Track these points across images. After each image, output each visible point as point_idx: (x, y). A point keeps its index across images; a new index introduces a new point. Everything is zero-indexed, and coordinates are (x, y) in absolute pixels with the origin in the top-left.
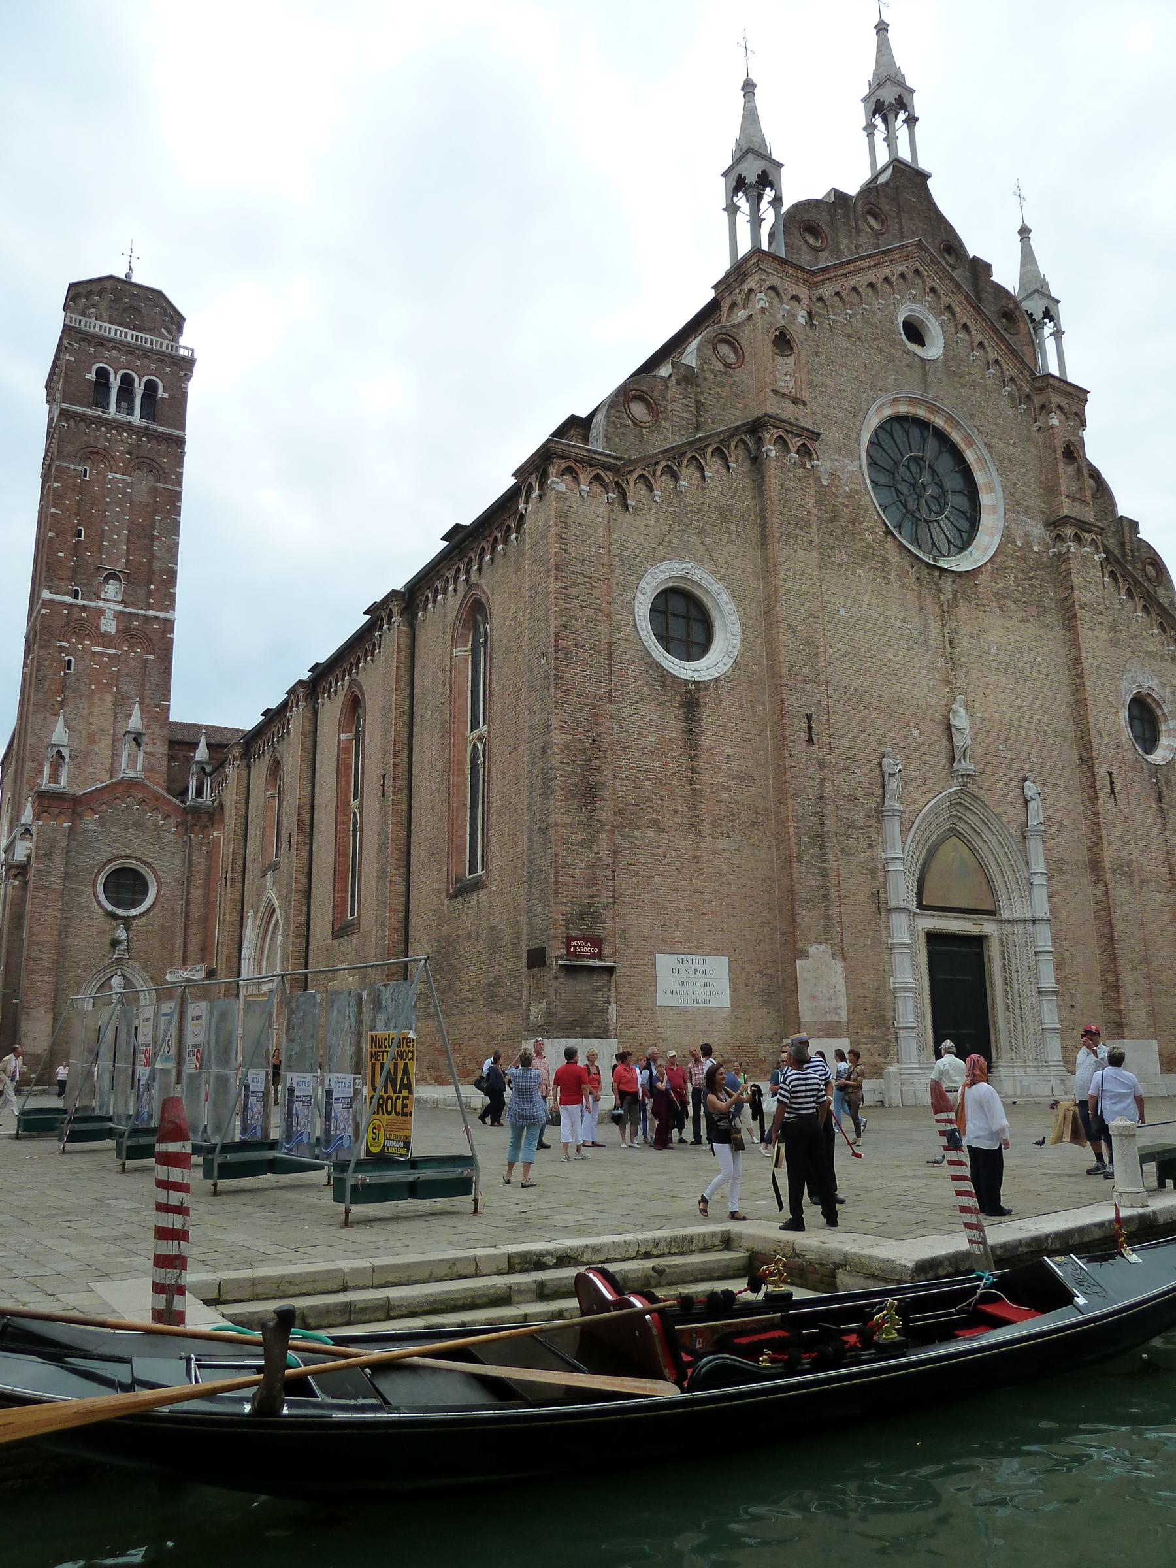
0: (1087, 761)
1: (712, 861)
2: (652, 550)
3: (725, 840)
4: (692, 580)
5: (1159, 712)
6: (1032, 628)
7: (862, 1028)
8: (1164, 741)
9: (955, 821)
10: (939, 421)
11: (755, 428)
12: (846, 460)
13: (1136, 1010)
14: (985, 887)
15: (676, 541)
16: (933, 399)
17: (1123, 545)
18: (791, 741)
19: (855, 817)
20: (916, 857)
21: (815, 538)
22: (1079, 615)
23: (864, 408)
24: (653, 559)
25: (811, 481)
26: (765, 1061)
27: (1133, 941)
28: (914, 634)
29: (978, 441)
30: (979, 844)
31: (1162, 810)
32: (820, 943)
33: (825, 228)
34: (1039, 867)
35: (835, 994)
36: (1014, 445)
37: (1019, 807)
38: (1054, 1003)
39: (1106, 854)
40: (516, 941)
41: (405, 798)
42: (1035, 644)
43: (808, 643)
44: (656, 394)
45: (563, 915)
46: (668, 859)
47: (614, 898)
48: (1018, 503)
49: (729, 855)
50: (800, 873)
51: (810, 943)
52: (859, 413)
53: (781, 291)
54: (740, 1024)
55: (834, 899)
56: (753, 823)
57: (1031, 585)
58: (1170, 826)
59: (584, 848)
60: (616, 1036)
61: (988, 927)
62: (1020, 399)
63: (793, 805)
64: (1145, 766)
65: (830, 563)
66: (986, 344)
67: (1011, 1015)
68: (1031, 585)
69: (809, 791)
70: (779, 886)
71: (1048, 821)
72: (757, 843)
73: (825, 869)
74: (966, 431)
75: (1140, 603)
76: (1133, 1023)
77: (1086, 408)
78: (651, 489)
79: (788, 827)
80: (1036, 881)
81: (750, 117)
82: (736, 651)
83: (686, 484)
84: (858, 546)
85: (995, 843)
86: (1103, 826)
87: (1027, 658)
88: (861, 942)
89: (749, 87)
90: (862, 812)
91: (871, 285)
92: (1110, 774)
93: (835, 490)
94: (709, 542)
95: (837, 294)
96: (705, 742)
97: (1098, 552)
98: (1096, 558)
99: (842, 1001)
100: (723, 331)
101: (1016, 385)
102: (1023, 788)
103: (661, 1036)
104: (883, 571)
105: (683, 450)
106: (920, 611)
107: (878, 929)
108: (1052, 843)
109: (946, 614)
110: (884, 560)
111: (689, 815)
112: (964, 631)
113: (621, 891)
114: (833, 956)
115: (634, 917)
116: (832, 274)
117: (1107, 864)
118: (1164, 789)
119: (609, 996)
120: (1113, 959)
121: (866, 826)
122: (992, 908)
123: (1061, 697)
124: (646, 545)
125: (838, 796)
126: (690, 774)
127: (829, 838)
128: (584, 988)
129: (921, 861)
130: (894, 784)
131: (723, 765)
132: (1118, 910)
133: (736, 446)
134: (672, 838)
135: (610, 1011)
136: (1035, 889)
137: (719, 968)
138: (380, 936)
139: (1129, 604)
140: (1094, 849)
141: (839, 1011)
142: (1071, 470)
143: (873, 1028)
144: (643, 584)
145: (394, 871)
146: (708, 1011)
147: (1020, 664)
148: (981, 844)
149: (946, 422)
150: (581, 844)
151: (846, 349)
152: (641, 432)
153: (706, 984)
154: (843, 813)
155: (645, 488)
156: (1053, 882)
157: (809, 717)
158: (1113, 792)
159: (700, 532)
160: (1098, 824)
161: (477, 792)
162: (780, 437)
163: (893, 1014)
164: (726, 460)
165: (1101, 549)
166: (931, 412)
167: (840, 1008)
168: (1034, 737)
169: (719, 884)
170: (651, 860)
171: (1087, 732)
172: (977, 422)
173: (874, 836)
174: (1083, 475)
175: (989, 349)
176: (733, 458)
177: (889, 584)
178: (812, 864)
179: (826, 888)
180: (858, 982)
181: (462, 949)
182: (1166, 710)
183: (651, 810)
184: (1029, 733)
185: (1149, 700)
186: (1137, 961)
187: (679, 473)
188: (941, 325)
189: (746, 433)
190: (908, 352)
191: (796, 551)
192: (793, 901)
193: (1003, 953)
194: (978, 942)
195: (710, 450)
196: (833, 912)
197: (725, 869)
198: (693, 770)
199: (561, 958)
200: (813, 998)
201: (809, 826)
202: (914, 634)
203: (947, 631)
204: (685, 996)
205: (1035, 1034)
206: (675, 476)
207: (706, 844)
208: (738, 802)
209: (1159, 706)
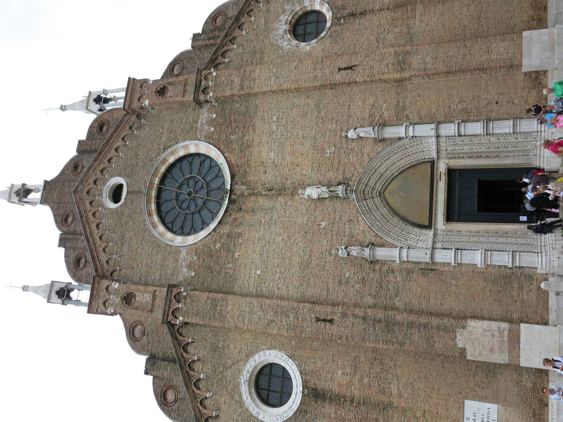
1: (405, 399)
2: (237, 403)
4: (250, 378)
5: (300, 13)
6: (258, 123)
7: (512, 297)
8: (317, 7)
10: (157, 181)
11: (171, 326)
12: (181, 256)
14: (415, 170)
15: (231, 385)
16: (146, 189)
17: (206, 46)
18: (332, 336)
21: (221, 295)
22: (247, 92)
23: (155, 239)
24: (241, 403)
25: (192, 293)
26: (534, 383)
27: (450, 53)
28: (268, 217)
29: (163, 156)
30: (388, 174)
32: (456, 337)
33: (76, 254)
35: (490, 331)
36: (163, 128)
37: (364, 142)
39: (391, 76)
42: (266, 121)
43: (276, 312)
44: (162, 383)
48: (192, 128)
49: (402, 384)
50: (411, 345)
51: (455, 345)
52: (158, 245)
53: (105, 299)
54: (508, 398)
56: (381, 363)
57: (235, 122)
58: (371, 7)
61: (442, 167)
62: (139, 122)
63: (369, 342)
64: (333, 29)
65: (234, 277)
66: (115, 146)
67: (503, 154)
68: (235, 122)
69: (361, 328)
72: (393, 362)
73: (408, 325)
74: (159, 164)
75: (237, 32)
76: (510, 55)
77: (138, 79)
78: (206, 398)
80: (411, 134)
81: (36, 290)
82: (285, 356)
83: (202, 375)
84: (223, 254)
85: (388, 162)
87: (275, 128)
88: (454, 289)
89: (25, 288)
90: (372, 275)
91: (97, 226)
92: (340, 69)
93: (197, 267)
94: (229, 362)
95: (104, 250)
96: (335, 389)
97: (211, 73)
98: (214, 74)
99: (494, 325)
100: (128, 333)
101: (133, 125)
102: (352, 139)
104: (235, 237)
105: (186, 374)
106: (254, 212)
107: (445, 273)
109: (256, 191)
110: (229, 236)
111: (378, 411)
112: (263, 178)
114: (464, 328)
116: (95, 254)
117: (398, 76)
118: (347, 11)
121: (380, 274)
122: (429, 164)
123: (295, 100)
124: (234, 406)
125: (363, 293)
126: (354, 404)
127: (388, 317)
131: (349, 378)
133: (181, 335)
136: (416, 134)
139: (239, 40)
141: (502, 329)
142: (170, 88)
143: (512, 287)
144: (254, 413)
147: (279, 134)
148: (388, 172)
149: (156, 176)
151: (128, 247)
152: (181, 399)
155: (206, 401)
156: (411, 116)
157: (318, 320)
158: (350, 68)
159: (225, 368)
162: (172, 313)
163: (503, 269)
164: (188, 344)
165: (209, 71)
166: (153, 187)
167: (499, 328)
168: (321, 125)
169: (419, 396)
171: (315, 87)
172: (153, 156)
173: (386, 267)
174: (172, 82)
175: (118, 144)
176: (187, 339)
177: (241, 234)
178: (405, 334)
179: (420, 325)
180: (481, 296)
182: (299, 8)
184: (318, 130)
185: (294, 21)
187: (198, 378)
188: (111, 177)
189: (173, 327)
190: (125, 203)
191: (228, 312)
193: (459, 158)
194: (451, 172)
195: (184, 354)
197: (409, 390)
201: (382, 332)
202: (268, 217)
203: (263, 193)
205: (517, 138)
206: (199, 380)
207: (395, 401)
208: (370, 372)
209: (296, 13)
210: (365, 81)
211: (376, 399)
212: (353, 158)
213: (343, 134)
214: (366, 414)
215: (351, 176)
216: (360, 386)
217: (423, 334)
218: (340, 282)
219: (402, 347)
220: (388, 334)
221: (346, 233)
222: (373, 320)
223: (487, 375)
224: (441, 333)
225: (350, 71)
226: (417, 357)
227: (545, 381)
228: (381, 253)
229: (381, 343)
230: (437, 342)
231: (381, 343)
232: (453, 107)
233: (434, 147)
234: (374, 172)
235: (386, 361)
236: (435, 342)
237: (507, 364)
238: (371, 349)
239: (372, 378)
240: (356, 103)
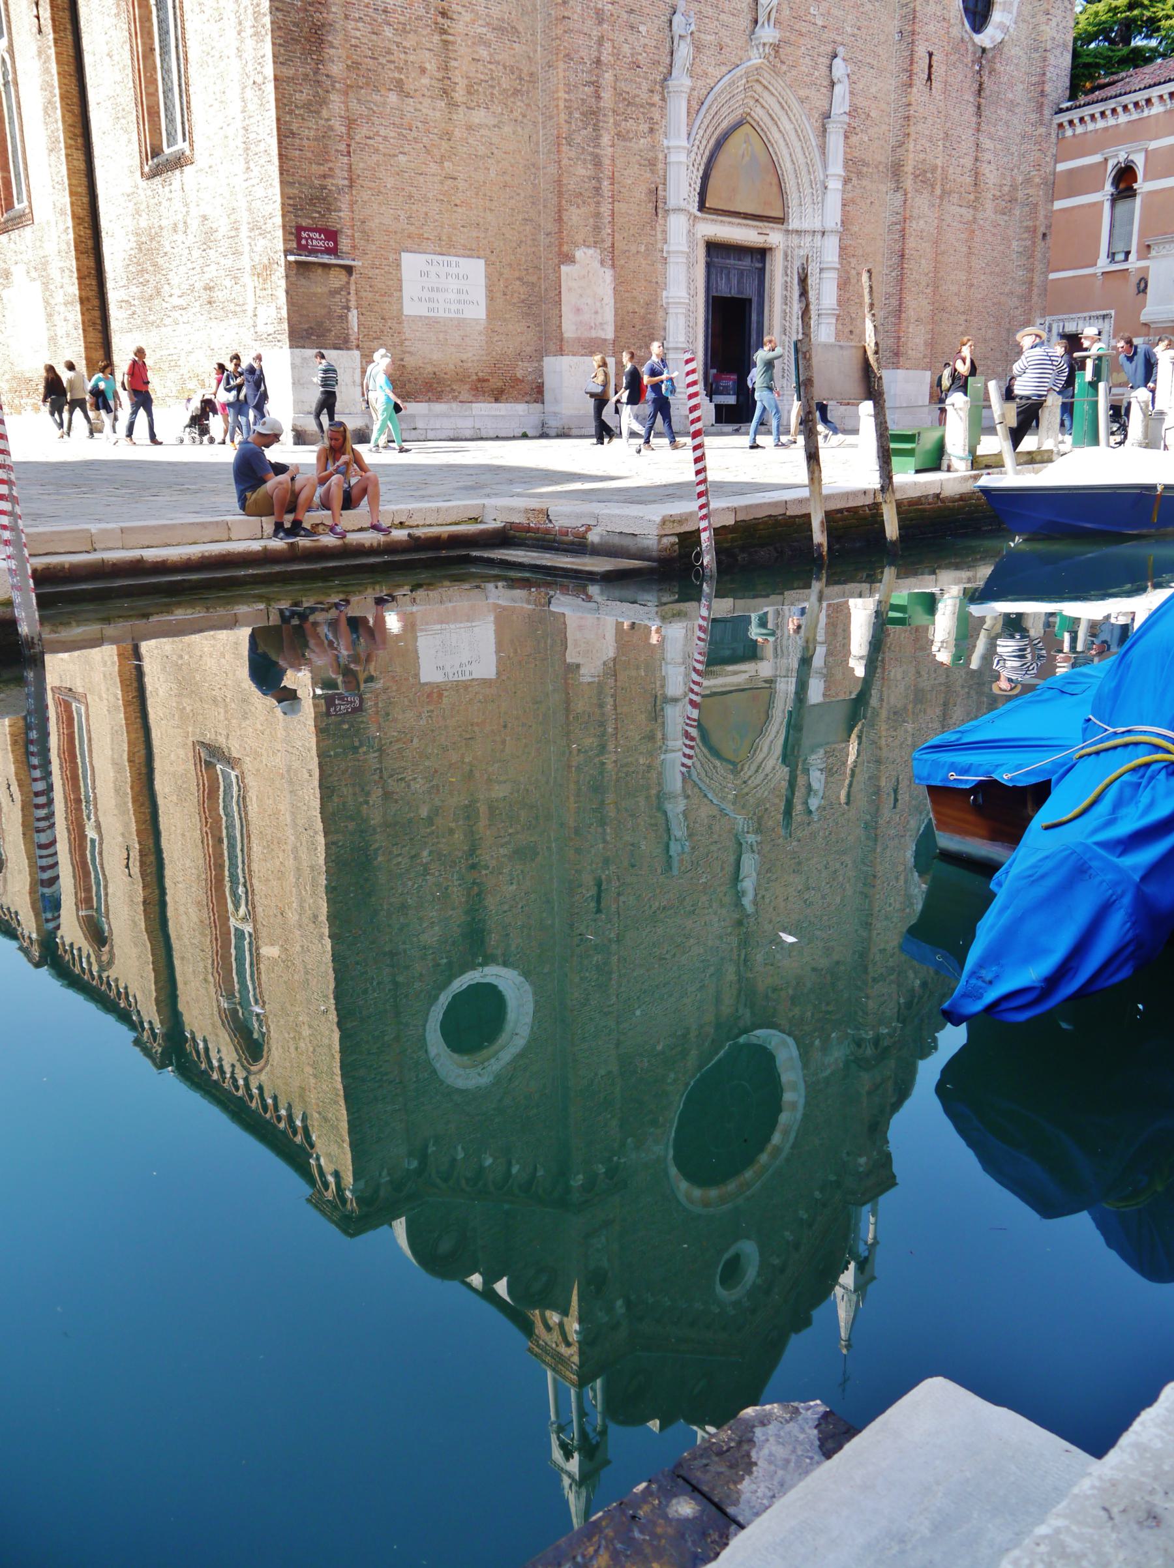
0: (908, 37)
3: (482, 112)
8: (997, 16)
9: (752, 103)
13: (916, 338)
14: (775, 189)
19: (637, 92)
20: (702, 148)
27: (923, 261)
30: (775, 135)
31: (979, 107)
32: (588, 247)
34: (837, 168)
37: (824, 90)
38: (833, 328)
39: (911, 156)
40: (233, 233)
41: (70, 37)
45: (289, 198)
46: (414, 134)
47: (351, 180)
50: (569, 159)
55: (607, 194)
56: (516, 92)
58: (984, 127)
59: (311, 112)
60: (358, 347)
61: (774, 238)
70: (545, 174)
71: (853, 112)
73: (597, 156)
79: (558, 99)
86: (913, 120)
88: (633, 249)
90: (645, 86)
92: (931, 55)
99: (608, 315)
102: (830, 67)
103: (408, 349)
108: (854, 139)
111: (440, 75)
113: (359, 172)
114: (602, 262)
115: (375, 206)
117: (909, 168)
118: (985, 78)
119: (348, 301)
120: (901, 279)
122: (779, 214)
126: (440, 20)
127: (605, 115)
128: (319, 290)
129: (707, 153)
130: (684, 51)
132: (914, 224)
134: (419, 106)
135: (350, 318)
136: (828, 192)
137: (475, 270)
138: (62, 227)
140: (898, 150)
145: (70, 141)
146: (461, 323)
148: (777, 135)
150: (307, 106)
153: (459, 292)
154: (622, 85)
156: (849, 187)
158: (929, 78)
160: (908, 118)
161: (167, 32)
169: (476, 170)
170: (393, 134)
173: (657, 117)
179: (599, 180)
180: (627, 295)
181: (167, 244)
183: (392, 66)
186: (924, 284)
192: (560, 194)
193: (786, 267)
194: (761, 253)
196: (605, 209)
197: (482, 150)
198: (444, 14)
199: (292, 254)
200: (578, 311)
204: (435, 305)
207: (460, 115)
210: (910, 105)
211: (457, 72)
212: (805, 65)
213: (841, 50)
214: (429, 46)
215: (783, 57)
216: (474, 37)
217: (586, 185)
218: (632, 11)
219: (564, 141)
220: (582, 114)
221: (702, 36)
222: (597, 82)
223: (523, 301)
224: (591, 220)
225: (926, 77)
226: (533, 170)
227: (528, 398)
228: (678, 108)
229: (566, 96)
230: (578, 211)
231: (566, 96)
232: (853, 261)
233: (806, 226)
234: (783, 108)
235: (519, 104)
236: (578, 207)
237: (562, 334)
238: (533, 69)
239: (490, 66)
240: (875, 81)
